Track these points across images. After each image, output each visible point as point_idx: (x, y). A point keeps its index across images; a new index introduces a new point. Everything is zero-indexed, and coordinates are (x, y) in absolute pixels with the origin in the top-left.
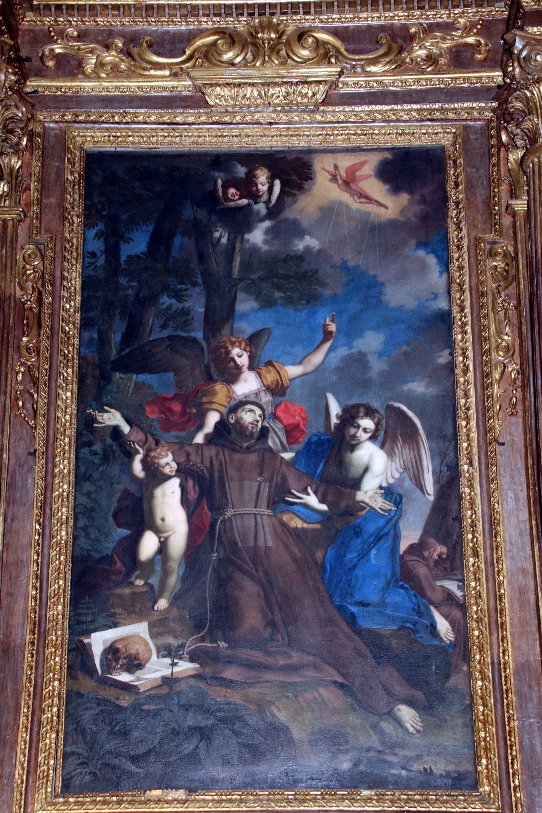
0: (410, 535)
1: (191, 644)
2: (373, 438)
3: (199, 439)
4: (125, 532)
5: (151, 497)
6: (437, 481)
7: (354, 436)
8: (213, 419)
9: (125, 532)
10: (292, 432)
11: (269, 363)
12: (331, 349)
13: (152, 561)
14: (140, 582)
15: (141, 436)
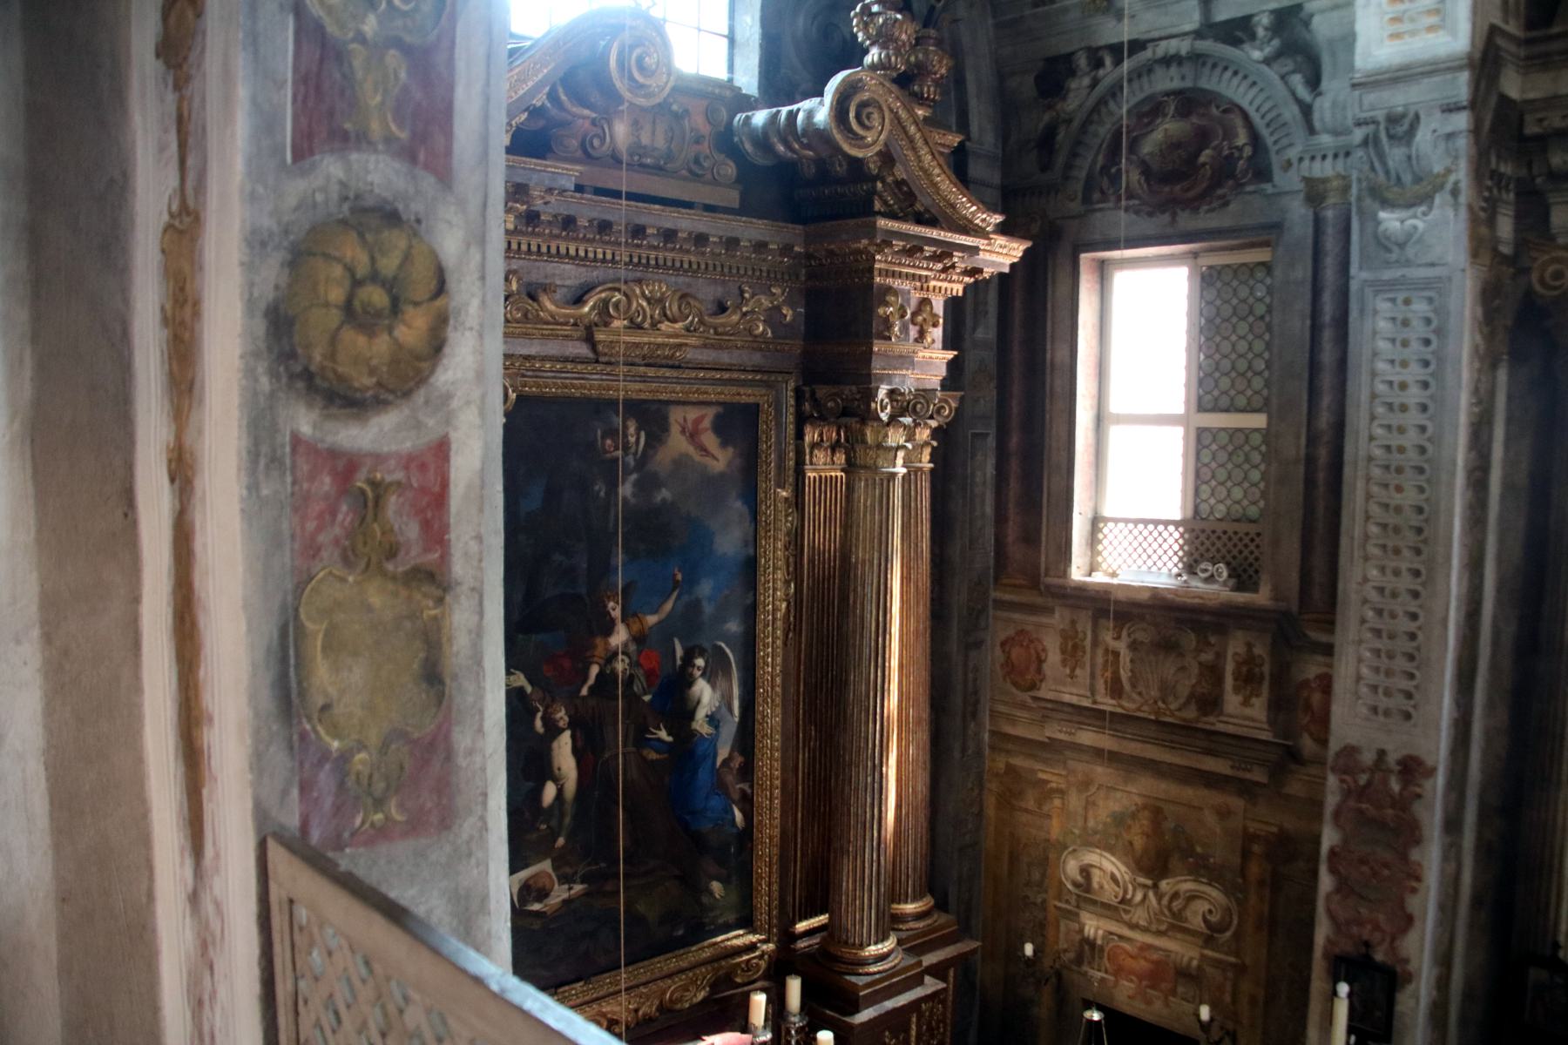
0: (723, 753)
1: (582, 870)
2: (703, 675)
3: (584, 691)
4: (531, 784)
5: (549, 749)
6: (741, 707)
7: (691, 675)
8: (594, 670)
9: (531, 784)
10: (650, 674)
11: (635, 615)
12: (678, 598)
13: (551, 806)
14: (544, 827)
15: (540, 694)
